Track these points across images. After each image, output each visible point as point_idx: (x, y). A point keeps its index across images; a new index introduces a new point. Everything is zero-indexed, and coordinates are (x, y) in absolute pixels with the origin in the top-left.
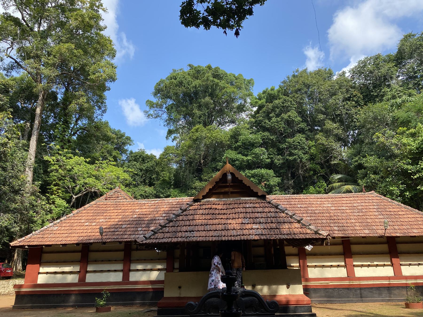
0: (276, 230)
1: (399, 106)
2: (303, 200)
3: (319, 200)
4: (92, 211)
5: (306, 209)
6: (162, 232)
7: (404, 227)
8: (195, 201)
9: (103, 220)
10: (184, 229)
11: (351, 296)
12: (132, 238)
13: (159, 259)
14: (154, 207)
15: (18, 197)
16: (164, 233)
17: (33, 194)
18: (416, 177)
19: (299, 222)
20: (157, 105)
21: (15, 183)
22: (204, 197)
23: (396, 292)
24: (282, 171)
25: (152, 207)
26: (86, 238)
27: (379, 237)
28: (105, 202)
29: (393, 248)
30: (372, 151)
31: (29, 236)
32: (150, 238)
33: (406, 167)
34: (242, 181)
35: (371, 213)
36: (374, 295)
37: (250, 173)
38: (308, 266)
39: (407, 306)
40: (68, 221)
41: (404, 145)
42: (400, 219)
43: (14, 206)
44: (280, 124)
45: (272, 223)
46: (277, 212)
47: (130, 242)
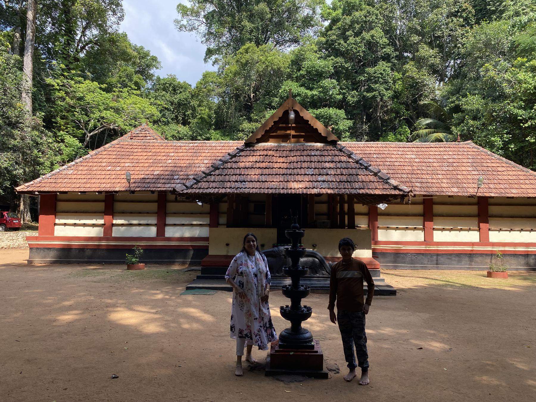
0: (346, 184)
1: (523, 27)
2: (381, 149)
3: (401, 149)
4: (115, 153)
5: (383, 160)
6: (207, 181)
7: (502, 186)
9: (129, 164)
10: (234, 178)
11: (426, 262)
12: (168, 187)
13: (200, 213)
14: (193, 151)
15: (16, 132)
16: (209, 182)
17: (34, 128)
18: (526, 125)
19: (375, 174)
20: (192, 11)
21: (12, 113)
22: (259, 141)
23: (479, 259)
24: (355, 112)
25: (190, 151)
26: (109, 185)
27: (469, 197)
28: (131, 142)
29: (483, 210)
30: (475, 90)
31: (38, 180)
32: (191, 187)
33: (516, 111)
34: (308, 121)
35: (463, 168)
36: (453, 262)
37: (314, 114)
38: (378, 227)
39: (489, 275)
41: (520, 82)
42: (499, 176)
43: (13, 142)
44: (359, 47)
45: (342, 175)
46: (349, 162)
47: (165, 192)
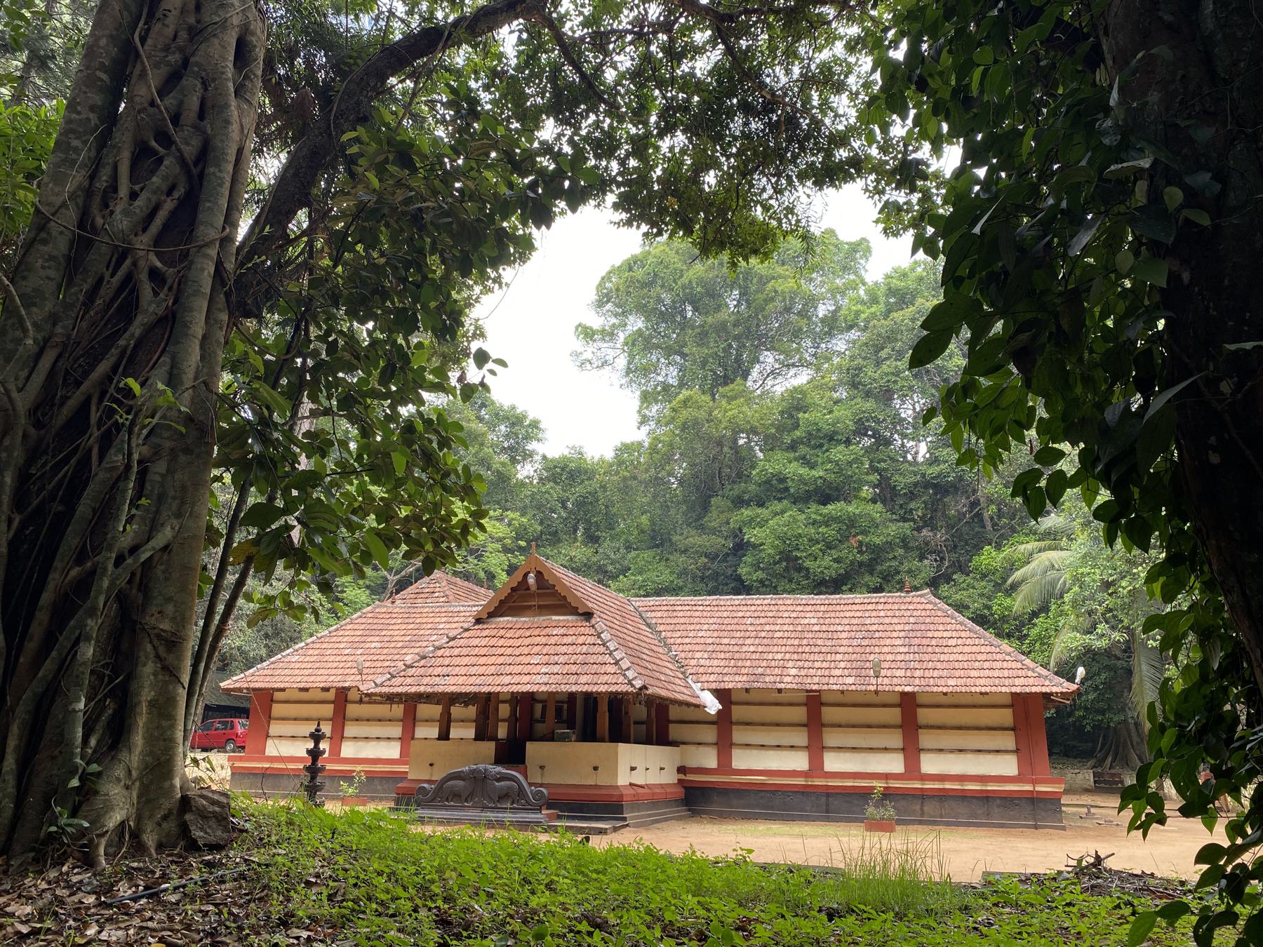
8: (478, 621)
19: (617, 663)
22: (491, 615)
24: (912, 505)
29: (910, 716)
31: (251, 671)
32: (382, 685)
40: (318, 646)
